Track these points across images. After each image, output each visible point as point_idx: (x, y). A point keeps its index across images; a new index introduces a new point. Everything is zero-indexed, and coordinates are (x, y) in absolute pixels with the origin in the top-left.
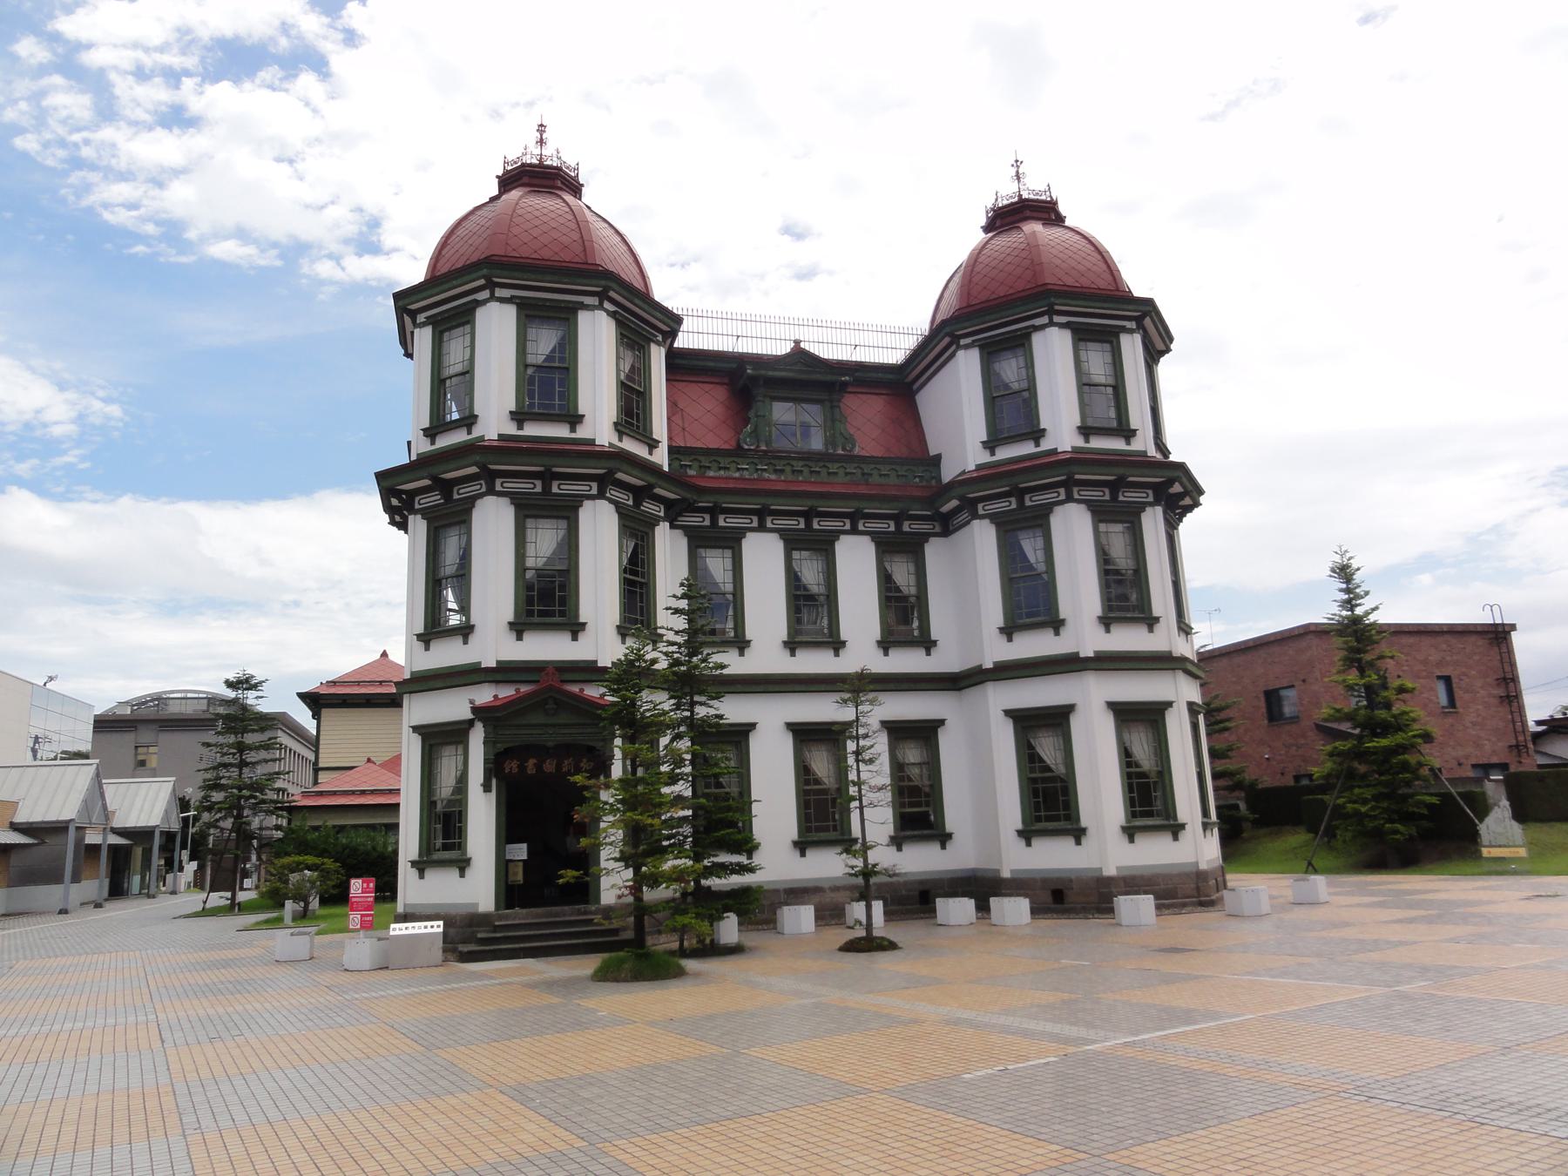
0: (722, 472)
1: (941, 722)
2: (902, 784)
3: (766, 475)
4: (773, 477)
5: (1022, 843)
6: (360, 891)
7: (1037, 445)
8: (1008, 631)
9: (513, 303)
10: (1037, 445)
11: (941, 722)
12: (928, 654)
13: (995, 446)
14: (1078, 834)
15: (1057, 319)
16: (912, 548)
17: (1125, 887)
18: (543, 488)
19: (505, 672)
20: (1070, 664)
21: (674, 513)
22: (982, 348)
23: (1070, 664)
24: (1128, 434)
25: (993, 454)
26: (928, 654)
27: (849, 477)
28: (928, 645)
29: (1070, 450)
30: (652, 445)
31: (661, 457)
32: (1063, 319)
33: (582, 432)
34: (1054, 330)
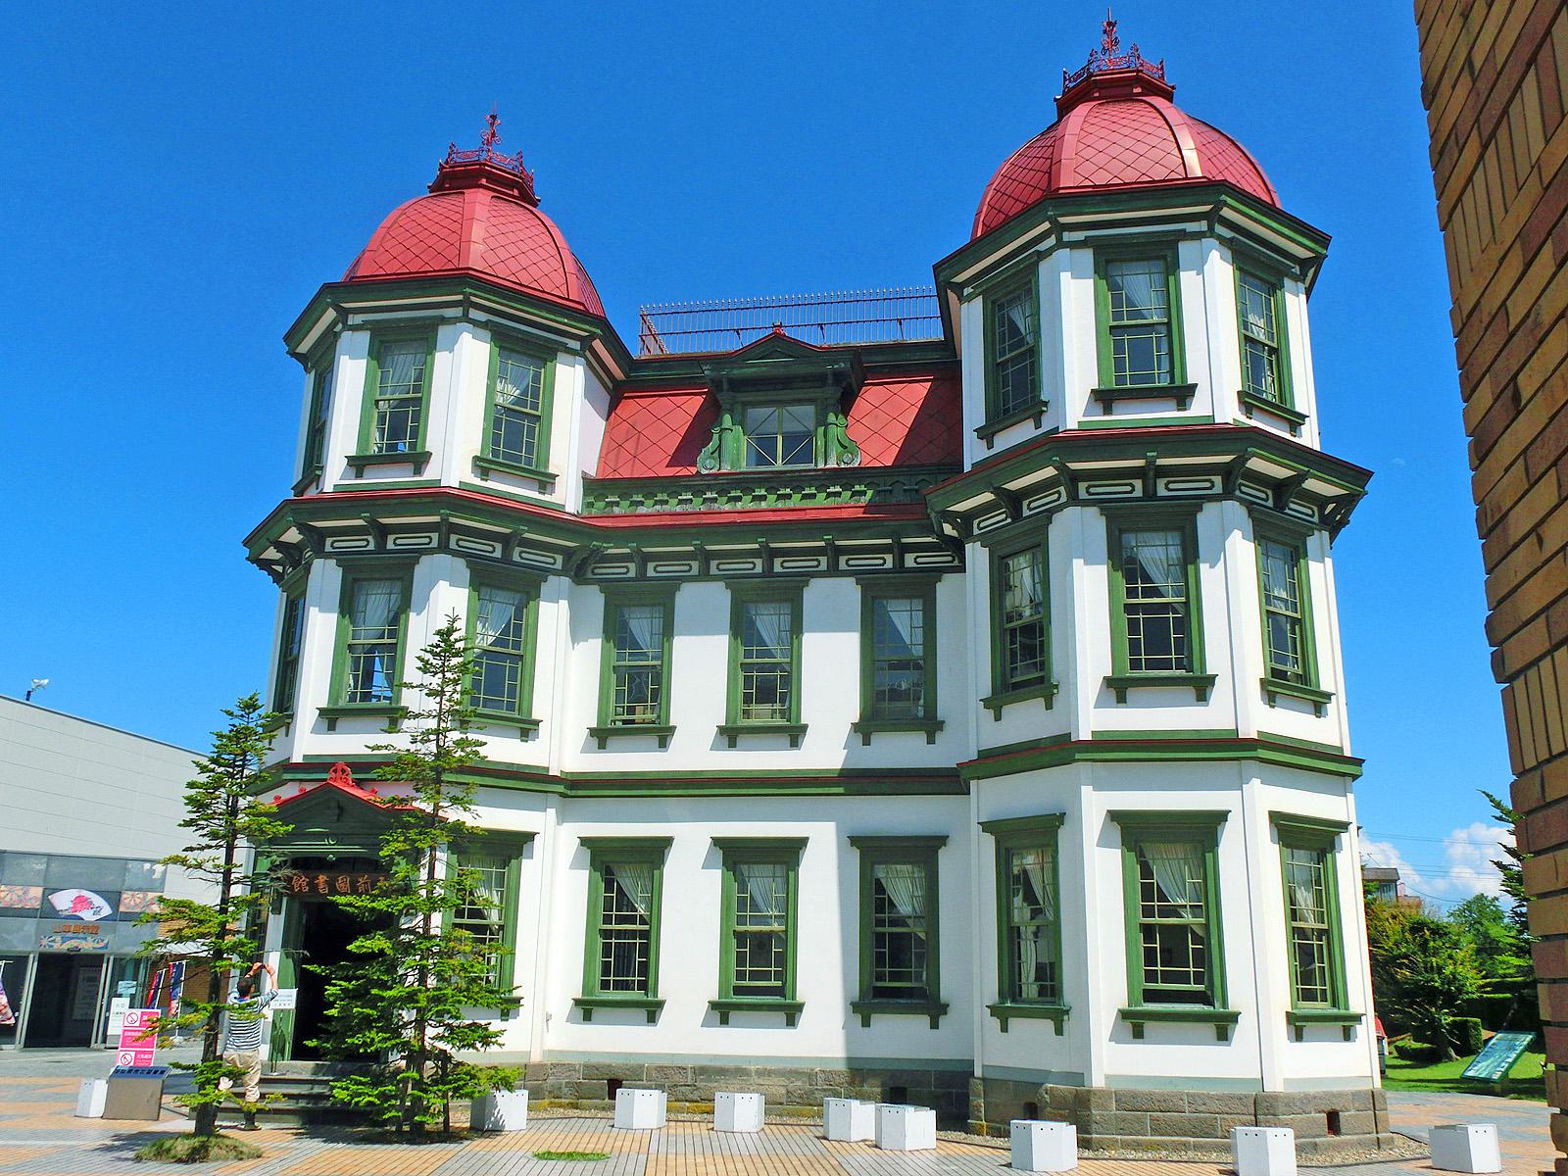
0: (658, 507)
1: (941, 840)
2: (880, 929)
3: (716, 506)
4: (727, 507)
5: (996, 1023)
6: (137, 1024)
7: (1038, 426)
8: (995, 704)
9: (367, 329)
10: (1038, 426)
11: (941, 840)
12: (931, 741)
13: (993, 434)
14: (1059, 1018)
15: (1067, 236)
16: (921, 587)
17: (1117, 1110)
18: (377, 544)
19: (313, 765)
20: (1060, 750)
21: (579, 570)
22: (983, 293)
23: (1060, 750)
24: (1183, 394)
25: (990, 446)
26: (931, 741)
27: (831, 499)
28: (931, 726)
29: (1076, 427)
30: (546, 481)
31: (568, 496)
32: (1080, 236)
33: (430, 473)
34: (1063, 254)
